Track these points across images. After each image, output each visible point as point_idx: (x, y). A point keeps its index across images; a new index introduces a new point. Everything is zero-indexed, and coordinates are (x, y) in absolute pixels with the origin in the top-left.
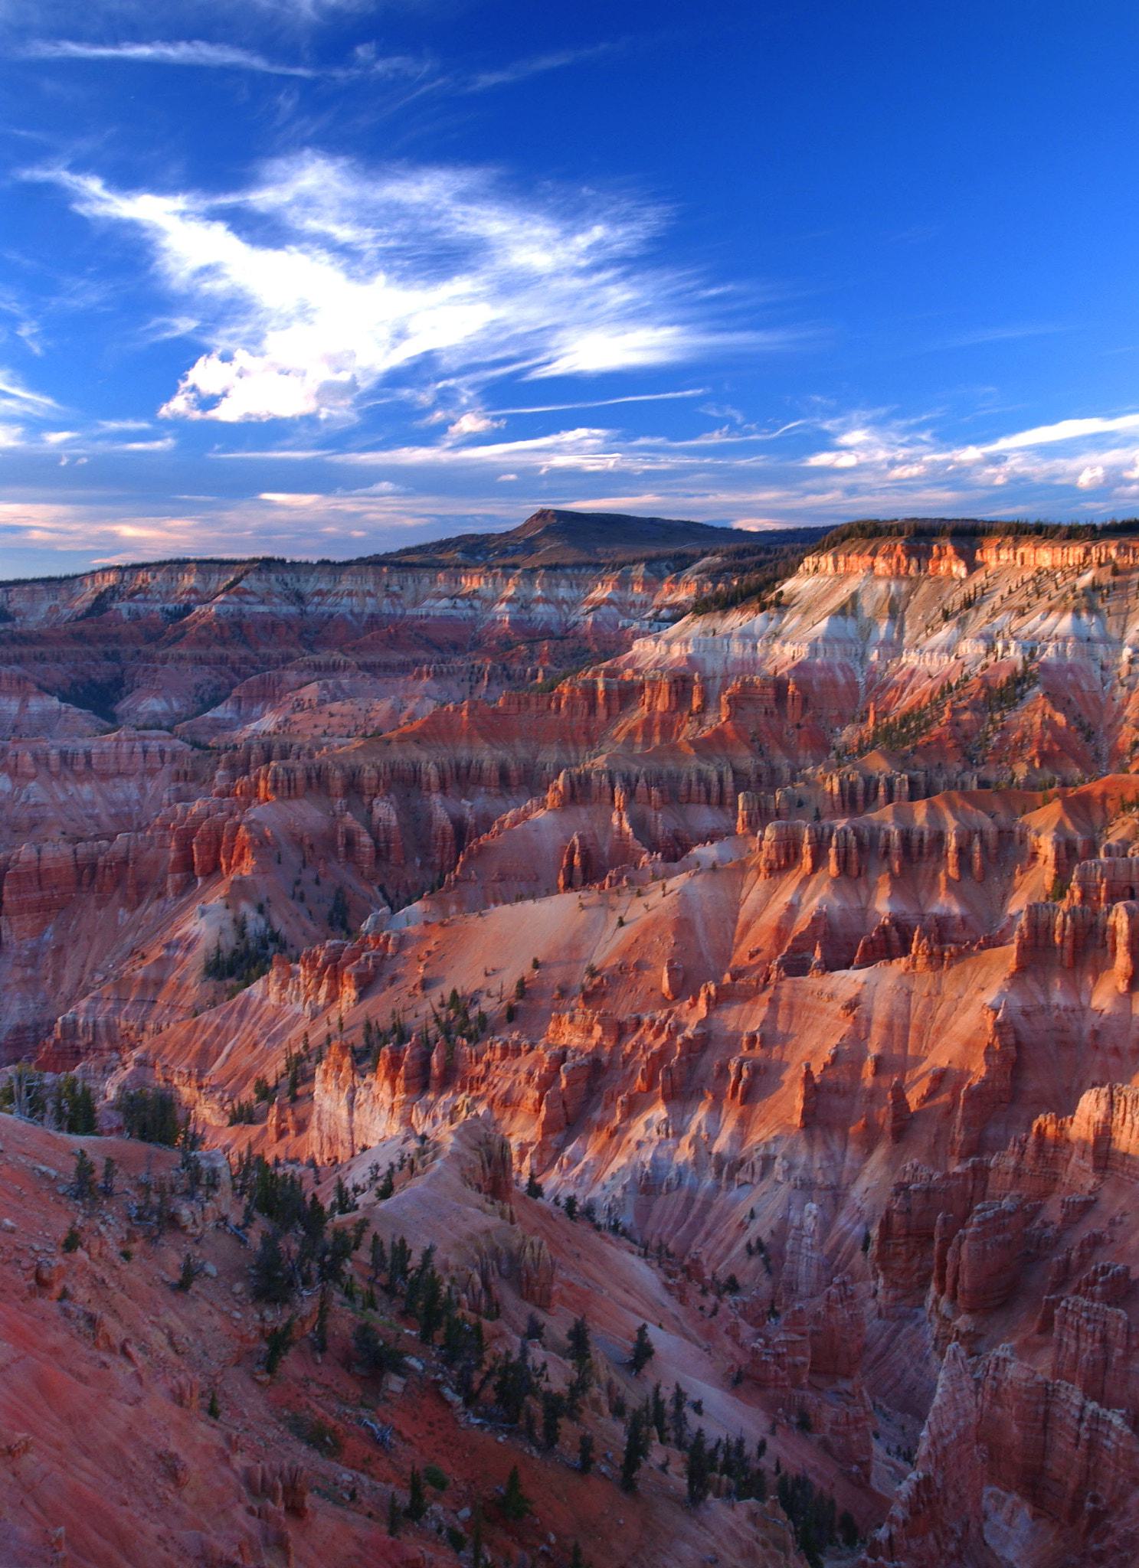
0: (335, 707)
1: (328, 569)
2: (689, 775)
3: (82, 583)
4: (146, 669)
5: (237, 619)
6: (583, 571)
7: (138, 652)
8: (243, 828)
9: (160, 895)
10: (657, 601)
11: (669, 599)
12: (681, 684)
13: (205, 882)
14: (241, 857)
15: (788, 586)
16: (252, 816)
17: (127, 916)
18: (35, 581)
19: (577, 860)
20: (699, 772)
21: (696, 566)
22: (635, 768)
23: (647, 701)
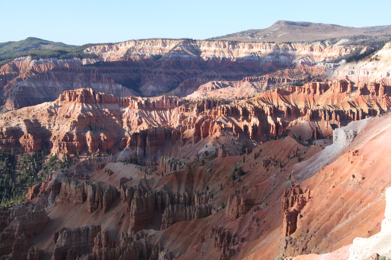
0: (222, 90)
1: (207, 42)
2: (348, 111)
3: (121, 45)
4: (149, 76)
5: (178, 59)
6: (298, 44)
7: (145, 70)
8: (216, 123)
9: (190, 142)
10: (324, 55)
11: (329, 55)
12: (344, 85)
13: (203, 138)
14: (215, 131)
15: (379, 53)
16: (218, 120)
17: (180, 148)
18: (105, 44)
19: (315, 134)
20: (351, 111)
21: (339, 43)
22: (331, 109)
23: (333, 89)
